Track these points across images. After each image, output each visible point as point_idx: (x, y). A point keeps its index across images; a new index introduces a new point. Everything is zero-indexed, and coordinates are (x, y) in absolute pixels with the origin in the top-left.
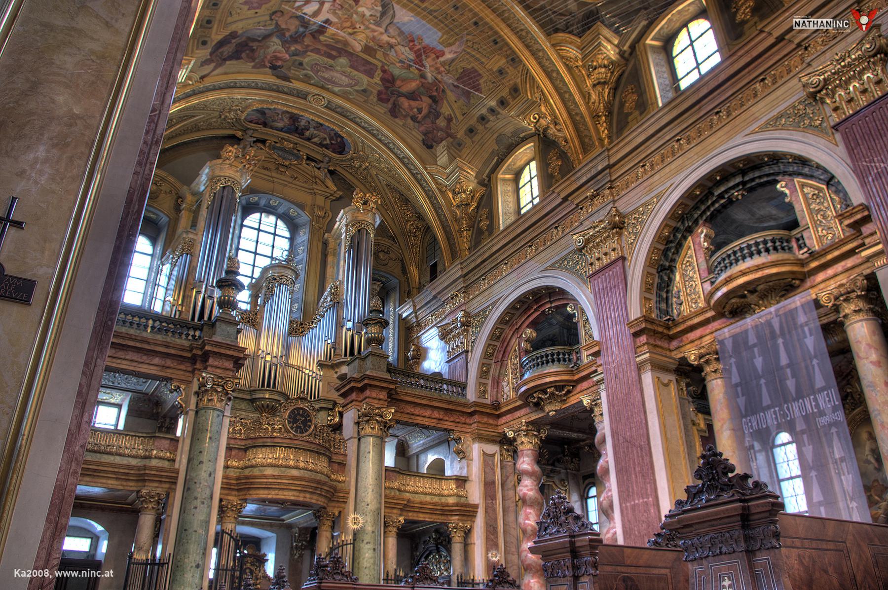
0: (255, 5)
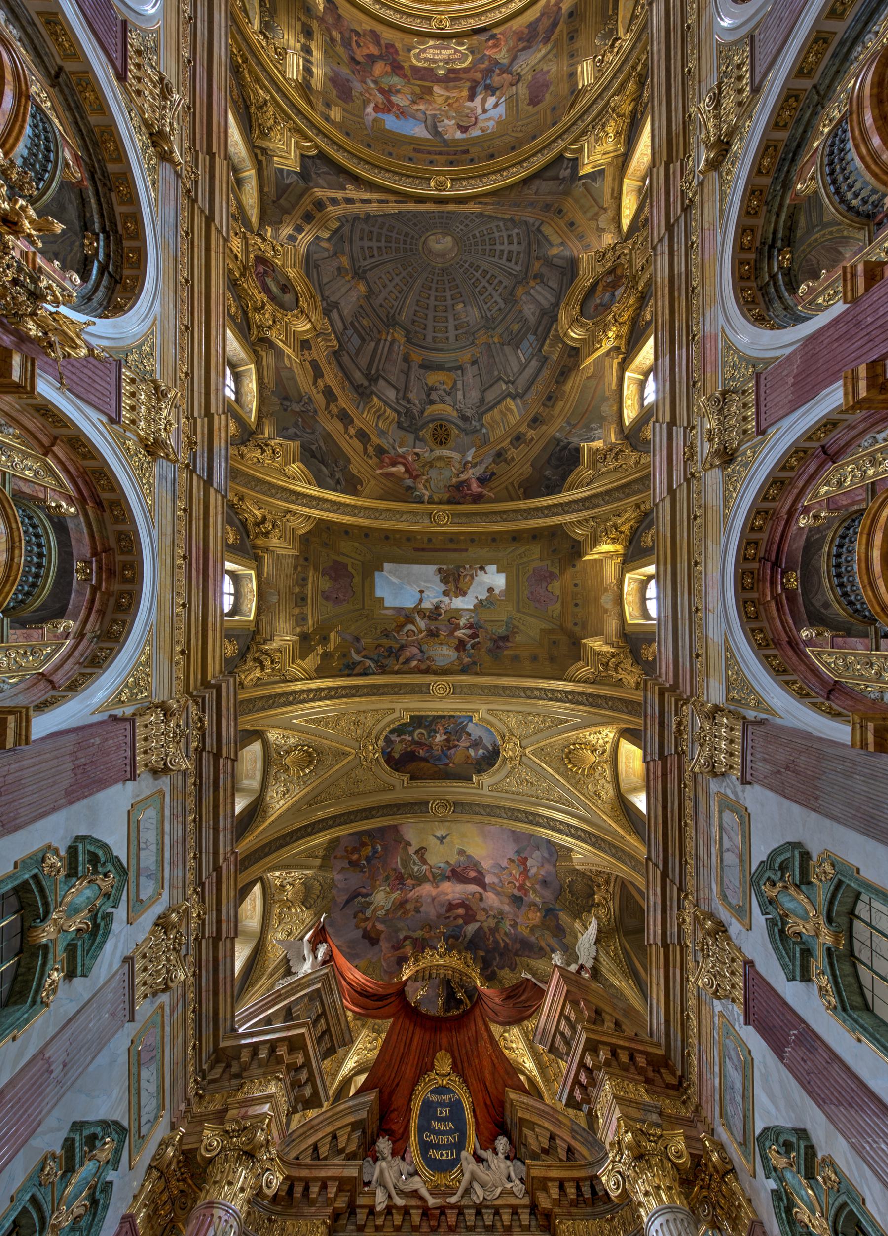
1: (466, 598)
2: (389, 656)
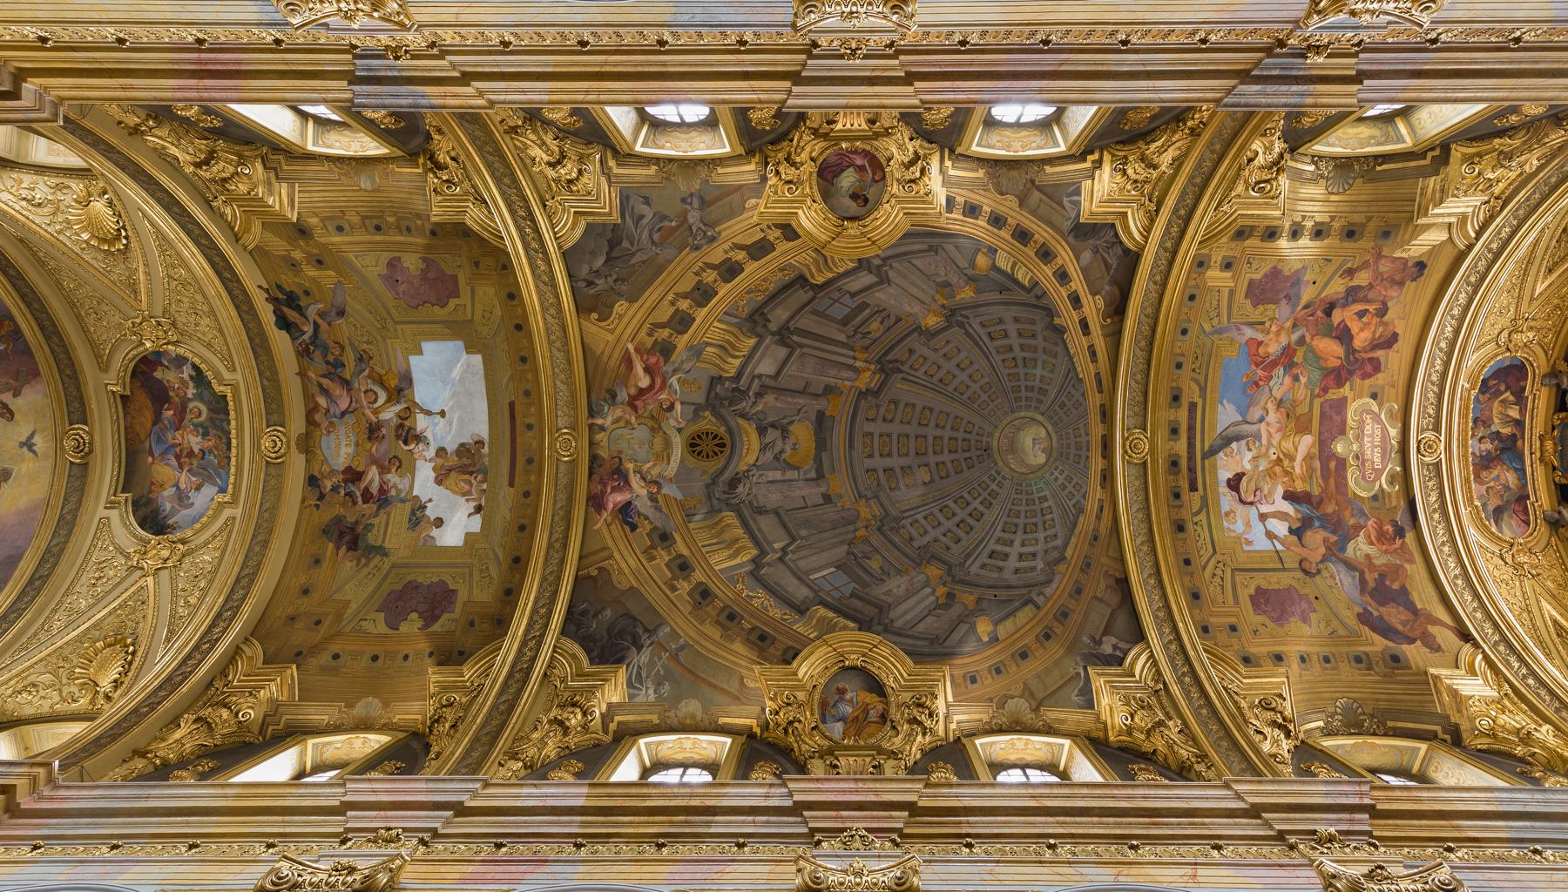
0: (1304, 605)
1: (431, 484)
2: (328, 363)
